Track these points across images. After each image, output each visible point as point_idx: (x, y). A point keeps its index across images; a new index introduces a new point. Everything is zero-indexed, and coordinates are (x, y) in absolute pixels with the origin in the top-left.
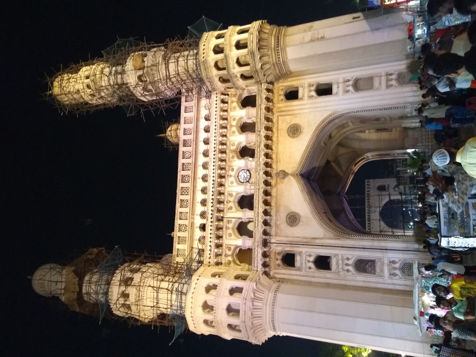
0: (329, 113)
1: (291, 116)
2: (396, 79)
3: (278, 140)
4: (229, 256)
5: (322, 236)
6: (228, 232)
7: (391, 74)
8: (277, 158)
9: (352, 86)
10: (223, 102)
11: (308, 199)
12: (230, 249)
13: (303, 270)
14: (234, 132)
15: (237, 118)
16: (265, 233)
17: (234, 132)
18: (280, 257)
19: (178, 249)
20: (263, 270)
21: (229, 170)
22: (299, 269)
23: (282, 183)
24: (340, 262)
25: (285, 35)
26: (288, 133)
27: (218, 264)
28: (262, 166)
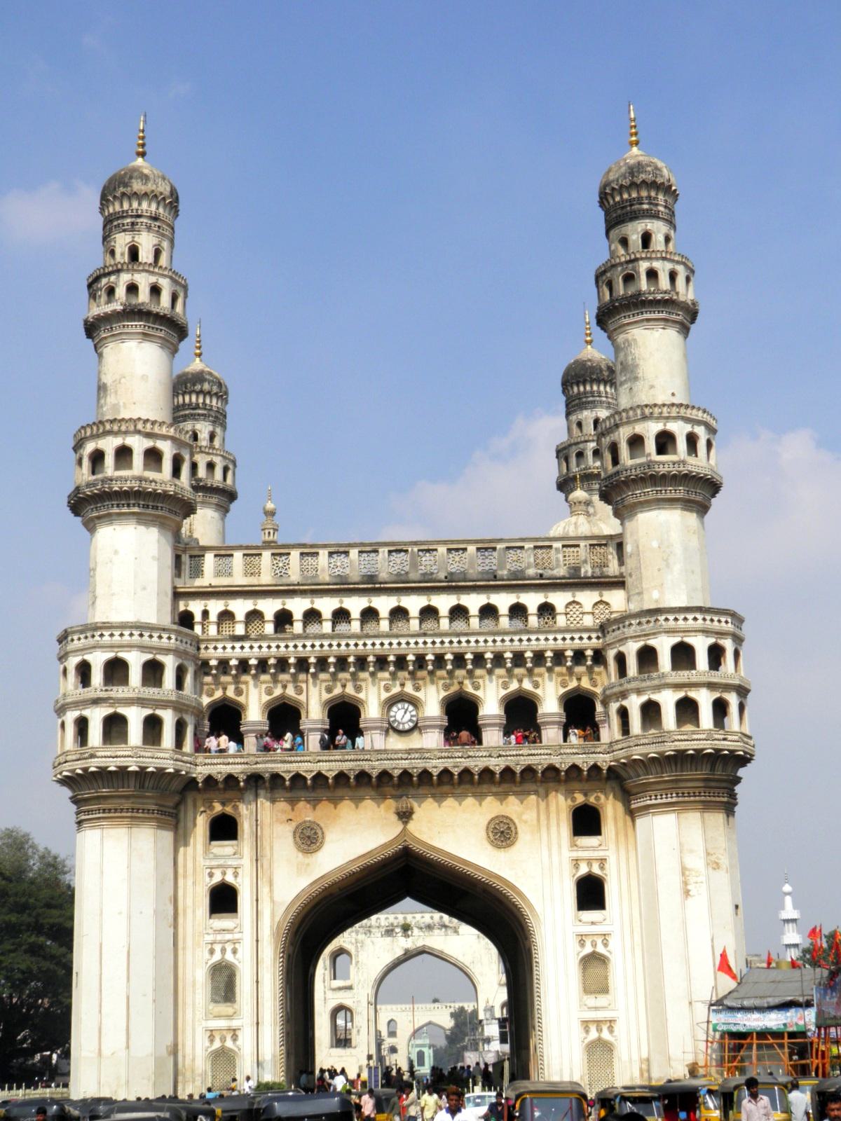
1: (535, 822)
2: (599, 1039)
4: (224, 693)
5: (277, 898)
7: (611, 1030)
9: (594, 953)
10: (579, 656)
11: (354, 868)
12: (239, 692)
14: (505, 686)
15: (539, 692)
16: (276, 777)
19: (232, 555)
20: (200, 779)
22: (206, 851)
24: (228, 937)
26: (497, 817)
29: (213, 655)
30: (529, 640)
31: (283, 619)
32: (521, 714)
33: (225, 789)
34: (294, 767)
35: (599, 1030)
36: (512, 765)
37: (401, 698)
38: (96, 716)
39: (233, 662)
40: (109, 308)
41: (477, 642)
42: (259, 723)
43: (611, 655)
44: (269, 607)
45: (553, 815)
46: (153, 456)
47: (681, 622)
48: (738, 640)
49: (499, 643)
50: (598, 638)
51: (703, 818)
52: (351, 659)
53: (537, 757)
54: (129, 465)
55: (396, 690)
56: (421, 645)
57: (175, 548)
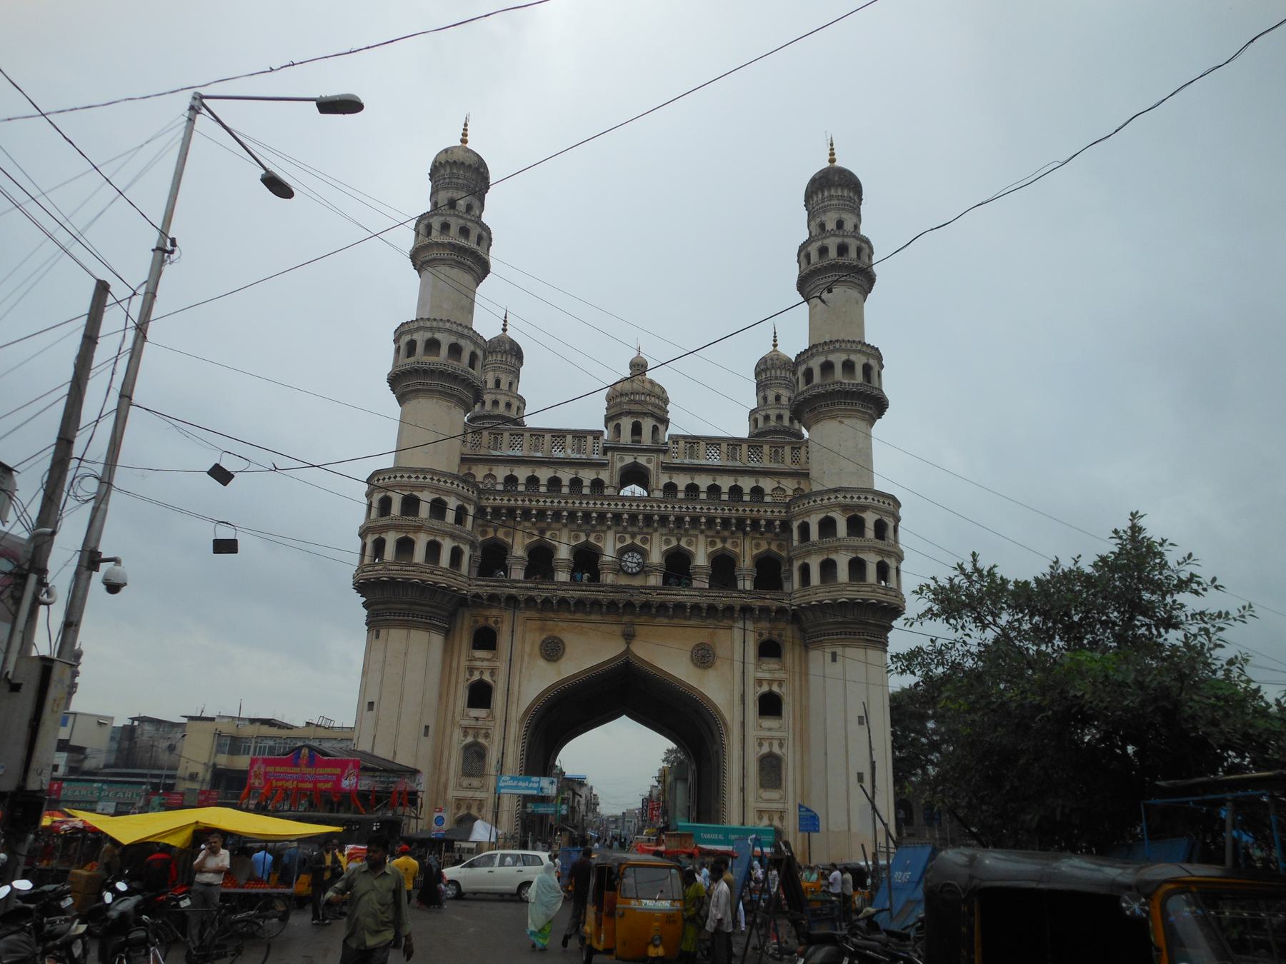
0: (727, 717)
14: (713, 543)
16: (530, 601)
17: (713, 543)
18: (491, 622)
27: (481, 511)
29: (489, 503)
32: (723, 568)
33: (490, 607)
37: (633, 548)
38: (391, 539)
42: (522, 558)
43: (795, 525)
46: (455, 350)
48: (897, 519)
52: (594, 515)
54: (438, 355)
55: (628, 541)
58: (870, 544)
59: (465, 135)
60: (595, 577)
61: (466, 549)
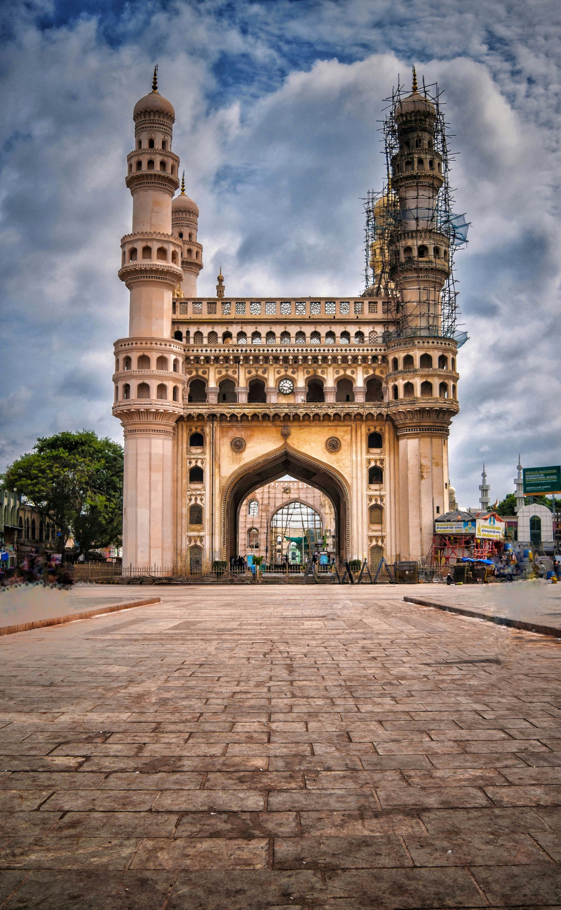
0: (349, 482)
3: (324, 426)
6: (222, 370)
7: (382, 541)
8: (304, 426)
10: (375, 358)
12: (204, 373)
13: (188, 456)
14: (338, 372)
15: (354, 376)
16: (222, 415)
17: (338, 372)
20: (185, 416)
21: (293, 368)
22: (188, 452)
23: (277, 432)
24: (199, 492)
25: (431, 437)
27: (187, 359)
28: (294, 411)
29: (192, 354)
30: (350, 350)
31: (227, 335)
32: (345, 386)
33: (197, 421)
34: (232, 411)
35: (377, 541)
36: (339, 412)
37: (286, 378)
38: (134, 385)
39: (202, 358)
40: (139, 173)
41: (324, 350)
43: (391, 358)
44: (220, 330)
45: (359, 438)
47: (426, 344)
48: (455, 353)
49: (335, 351)
50: (385, 350)
51: (431, 441)
53: (352, 409)
55: (283, 373)
56: (296, 351)
57: (173, 299)
58: (435, 373)
59: (155, 83)
60: (263, 399)
61: (180, 387)
